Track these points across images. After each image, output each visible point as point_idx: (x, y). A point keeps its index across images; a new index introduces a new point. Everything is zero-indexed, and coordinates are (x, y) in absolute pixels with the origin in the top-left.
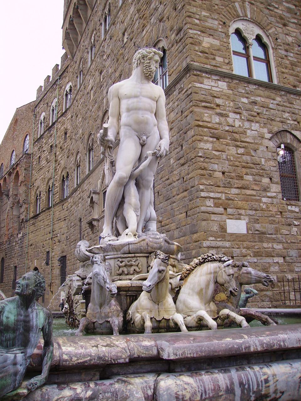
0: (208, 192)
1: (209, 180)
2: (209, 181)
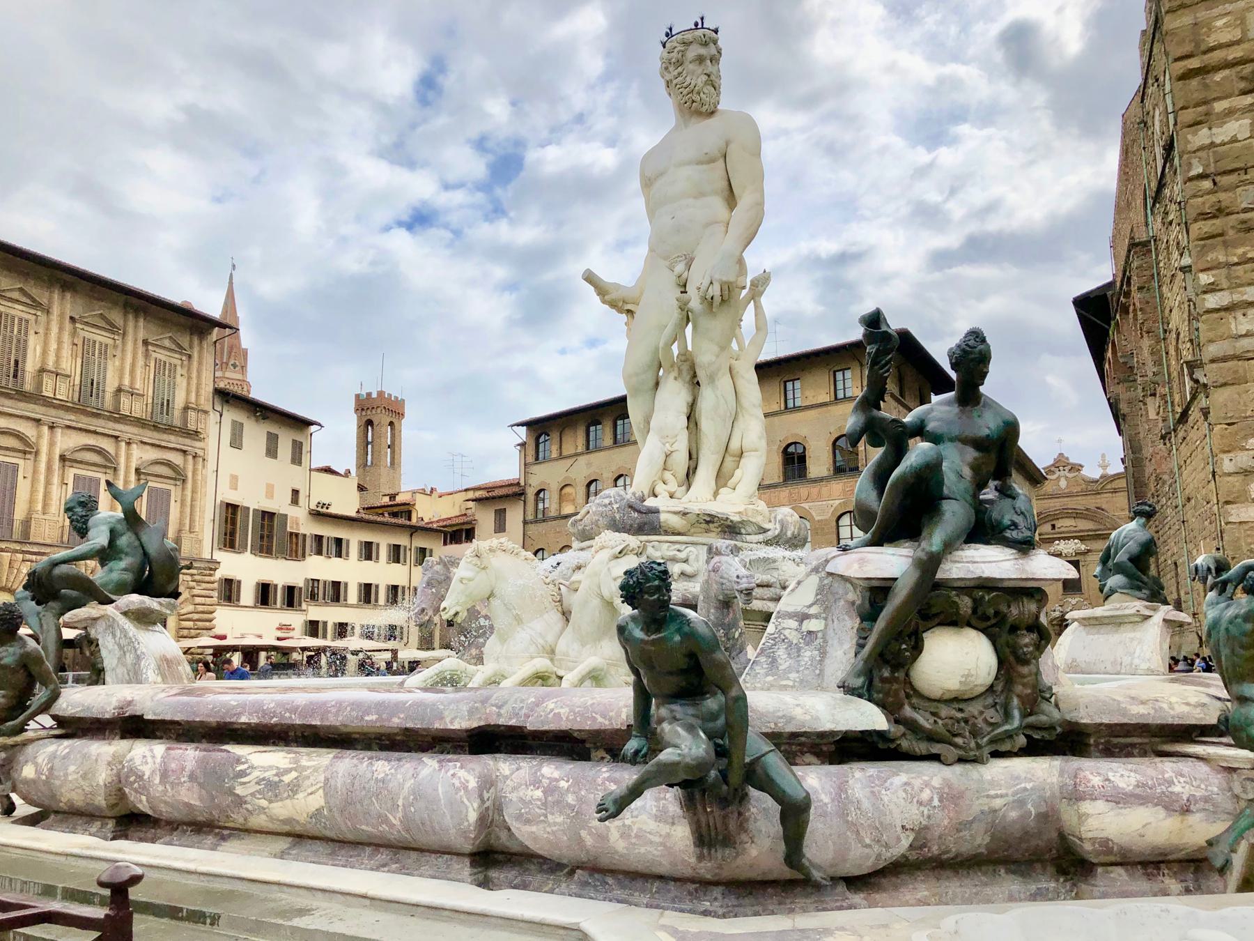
0: (1242, 285)
1: (1243, 245)
2: (1240, 251)
